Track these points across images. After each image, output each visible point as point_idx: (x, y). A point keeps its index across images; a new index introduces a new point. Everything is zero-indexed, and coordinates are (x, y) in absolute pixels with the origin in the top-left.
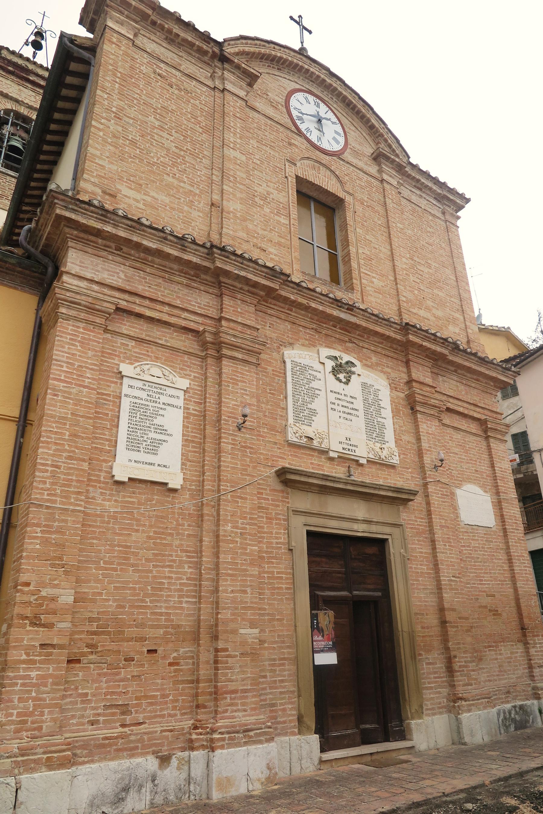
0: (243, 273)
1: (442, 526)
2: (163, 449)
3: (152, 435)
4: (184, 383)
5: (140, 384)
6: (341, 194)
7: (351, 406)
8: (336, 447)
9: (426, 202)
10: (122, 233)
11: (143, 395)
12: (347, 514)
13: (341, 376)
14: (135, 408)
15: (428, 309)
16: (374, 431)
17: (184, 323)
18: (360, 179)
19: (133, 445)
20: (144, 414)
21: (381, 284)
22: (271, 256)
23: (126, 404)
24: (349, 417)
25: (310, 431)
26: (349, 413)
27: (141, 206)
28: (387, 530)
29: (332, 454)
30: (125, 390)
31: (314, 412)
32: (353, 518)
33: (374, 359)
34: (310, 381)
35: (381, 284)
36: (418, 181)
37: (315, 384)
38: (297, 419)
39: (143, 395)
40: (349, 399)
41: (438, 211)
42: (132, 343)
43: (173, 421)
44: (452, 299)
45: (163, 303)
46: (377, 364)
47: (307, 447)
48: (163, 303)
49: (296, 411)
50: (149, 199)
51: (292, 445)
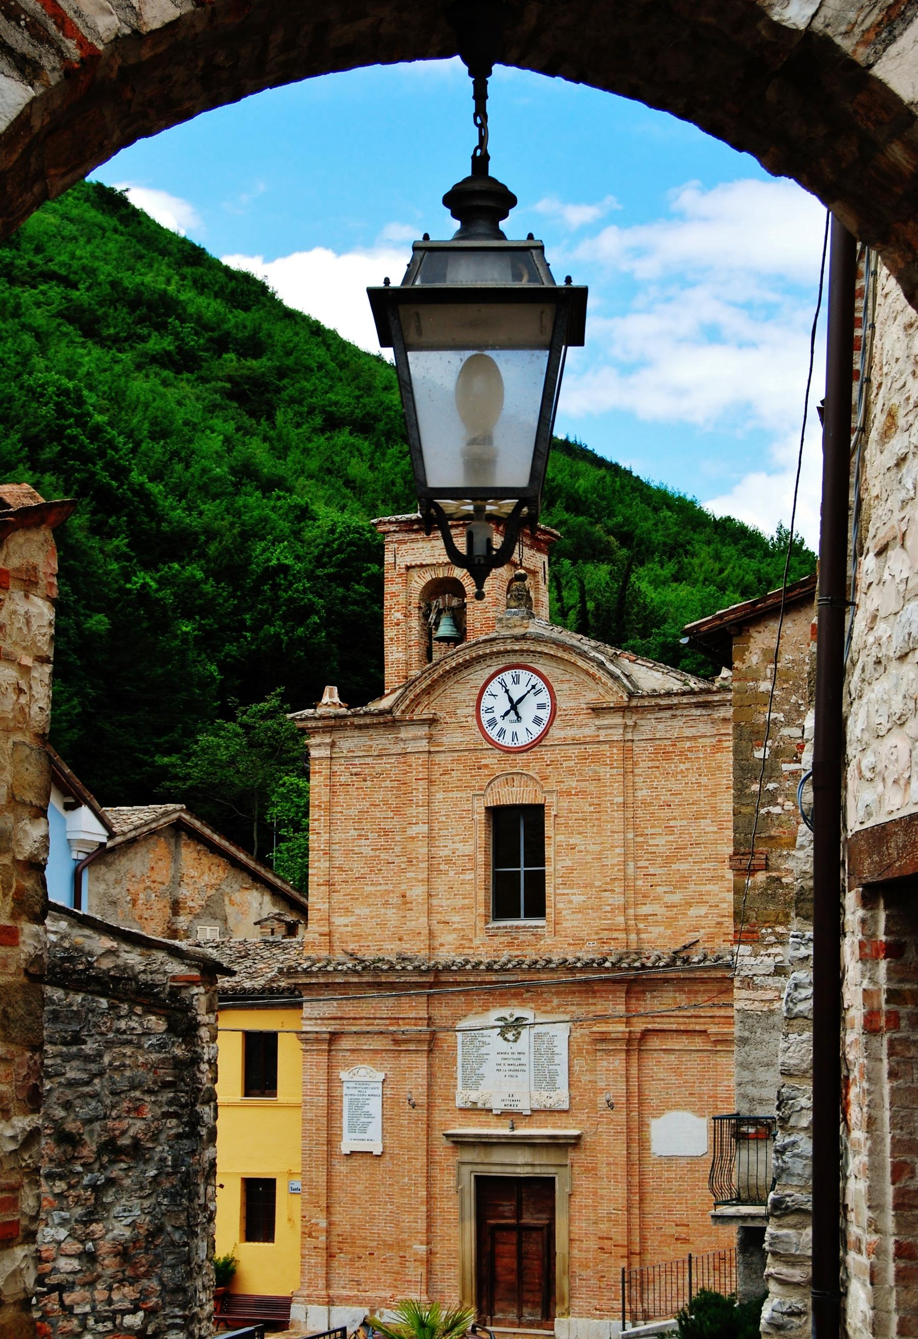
0: (403, 979)
1: (608, 1164)
2: (370, 1129)
3: (363, 1120)
4: (381, 1076)
5: (353, 1085)
6: (539, 801)
7: (518, 1062)
8: (497, 1105)
9: (684, 719)
10: (322, 980)
11: (355, 1092)
12: (507, 1161)
13: (510, 1036)
14: (351, 1101)
15: (657, 899)
16: (546, 1081)
17: (376, 1029)
18: (569, 758)
19: (352, 1130)
20: (357, 1105)
21: (583, 898)
22: (455, 926)
23: (346, 1100)
24: (515, 1073)
25: (474, 1096)
26: (516, 1069)
27: (349, 929)
28: (552, 1170)
29: (494, 1112)
30: (345, 1091)
31: (482, 1076)
32: (519, 1164)
33: (556, 1001)
34: (478, 1048)
35: (583, 898)
36: (657, 705)
37: (483, 1050)
38: (466, 1086)
39: (355, 1092)
40: (516, 1056)
41: (706, 722)
42: (348, 1054)
43: (375, 1107)
44: (704, 866)
45: (361, 1018)
46: (559, 1006)
47: (473, 1110)
48: (361, 1018)
49: (464, 1079)
50: (353, 919)
51: (461, 1109)
